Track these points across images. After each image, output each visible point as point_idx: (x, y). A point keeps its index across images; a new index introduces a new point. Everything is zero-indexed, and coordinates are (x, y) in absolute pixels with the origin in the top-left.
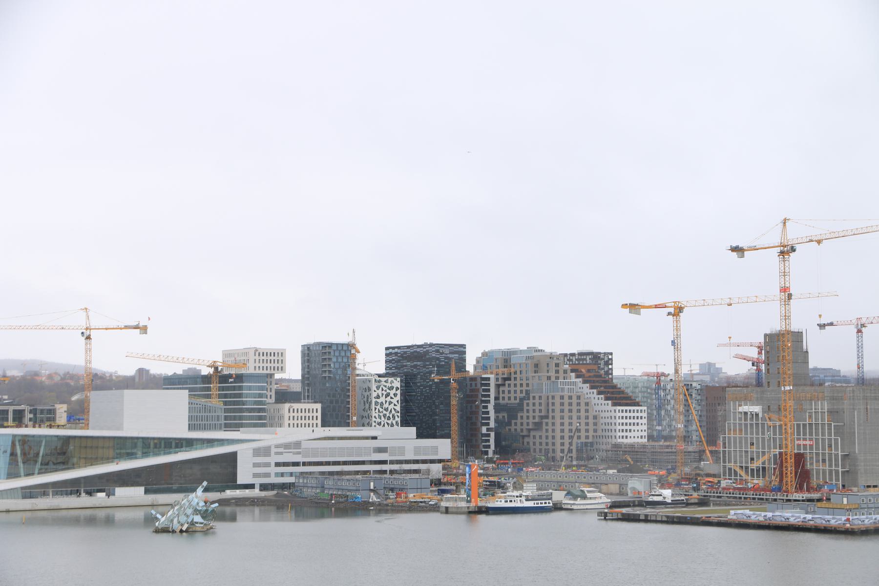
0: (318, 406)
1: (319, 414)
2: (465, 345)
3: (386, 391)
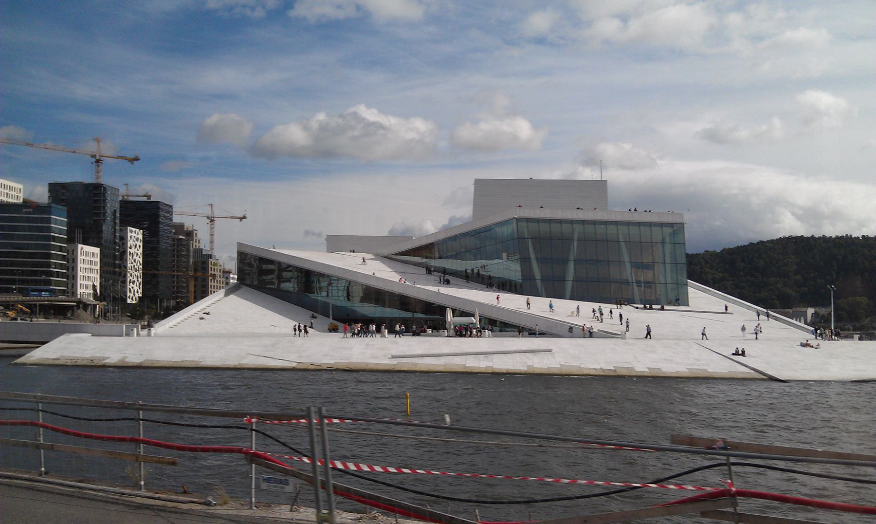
0: (97, 250)
1: (98, 260)
2: (172, 206)
3: (135, 242)
